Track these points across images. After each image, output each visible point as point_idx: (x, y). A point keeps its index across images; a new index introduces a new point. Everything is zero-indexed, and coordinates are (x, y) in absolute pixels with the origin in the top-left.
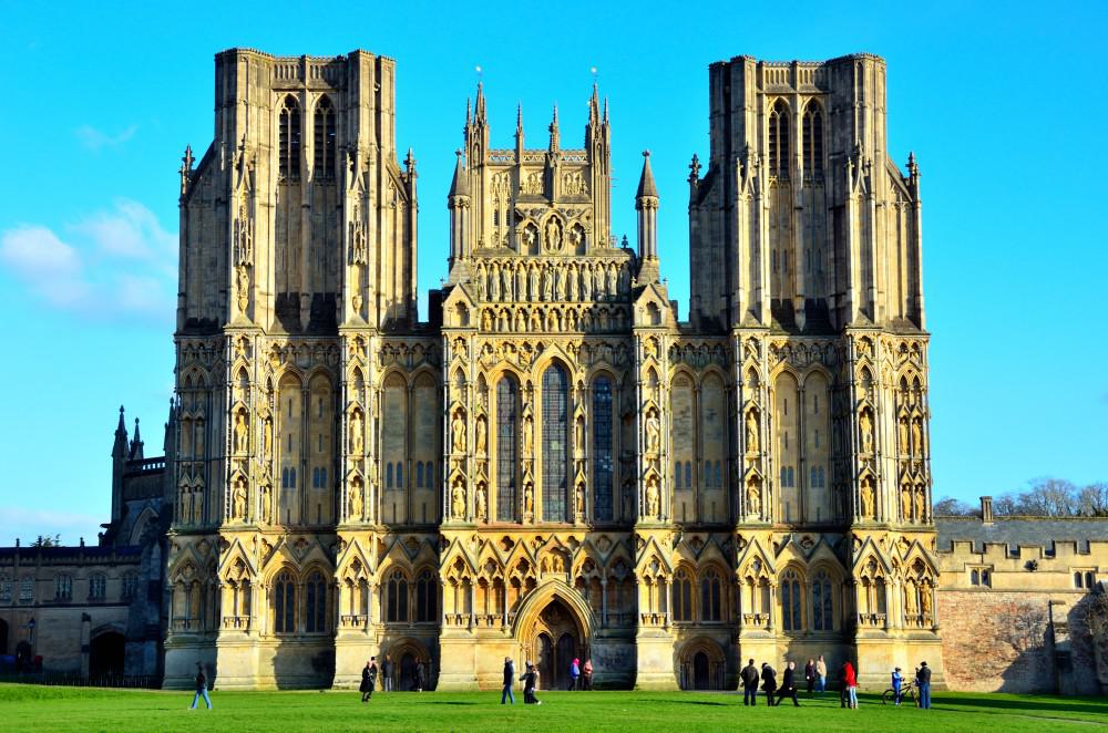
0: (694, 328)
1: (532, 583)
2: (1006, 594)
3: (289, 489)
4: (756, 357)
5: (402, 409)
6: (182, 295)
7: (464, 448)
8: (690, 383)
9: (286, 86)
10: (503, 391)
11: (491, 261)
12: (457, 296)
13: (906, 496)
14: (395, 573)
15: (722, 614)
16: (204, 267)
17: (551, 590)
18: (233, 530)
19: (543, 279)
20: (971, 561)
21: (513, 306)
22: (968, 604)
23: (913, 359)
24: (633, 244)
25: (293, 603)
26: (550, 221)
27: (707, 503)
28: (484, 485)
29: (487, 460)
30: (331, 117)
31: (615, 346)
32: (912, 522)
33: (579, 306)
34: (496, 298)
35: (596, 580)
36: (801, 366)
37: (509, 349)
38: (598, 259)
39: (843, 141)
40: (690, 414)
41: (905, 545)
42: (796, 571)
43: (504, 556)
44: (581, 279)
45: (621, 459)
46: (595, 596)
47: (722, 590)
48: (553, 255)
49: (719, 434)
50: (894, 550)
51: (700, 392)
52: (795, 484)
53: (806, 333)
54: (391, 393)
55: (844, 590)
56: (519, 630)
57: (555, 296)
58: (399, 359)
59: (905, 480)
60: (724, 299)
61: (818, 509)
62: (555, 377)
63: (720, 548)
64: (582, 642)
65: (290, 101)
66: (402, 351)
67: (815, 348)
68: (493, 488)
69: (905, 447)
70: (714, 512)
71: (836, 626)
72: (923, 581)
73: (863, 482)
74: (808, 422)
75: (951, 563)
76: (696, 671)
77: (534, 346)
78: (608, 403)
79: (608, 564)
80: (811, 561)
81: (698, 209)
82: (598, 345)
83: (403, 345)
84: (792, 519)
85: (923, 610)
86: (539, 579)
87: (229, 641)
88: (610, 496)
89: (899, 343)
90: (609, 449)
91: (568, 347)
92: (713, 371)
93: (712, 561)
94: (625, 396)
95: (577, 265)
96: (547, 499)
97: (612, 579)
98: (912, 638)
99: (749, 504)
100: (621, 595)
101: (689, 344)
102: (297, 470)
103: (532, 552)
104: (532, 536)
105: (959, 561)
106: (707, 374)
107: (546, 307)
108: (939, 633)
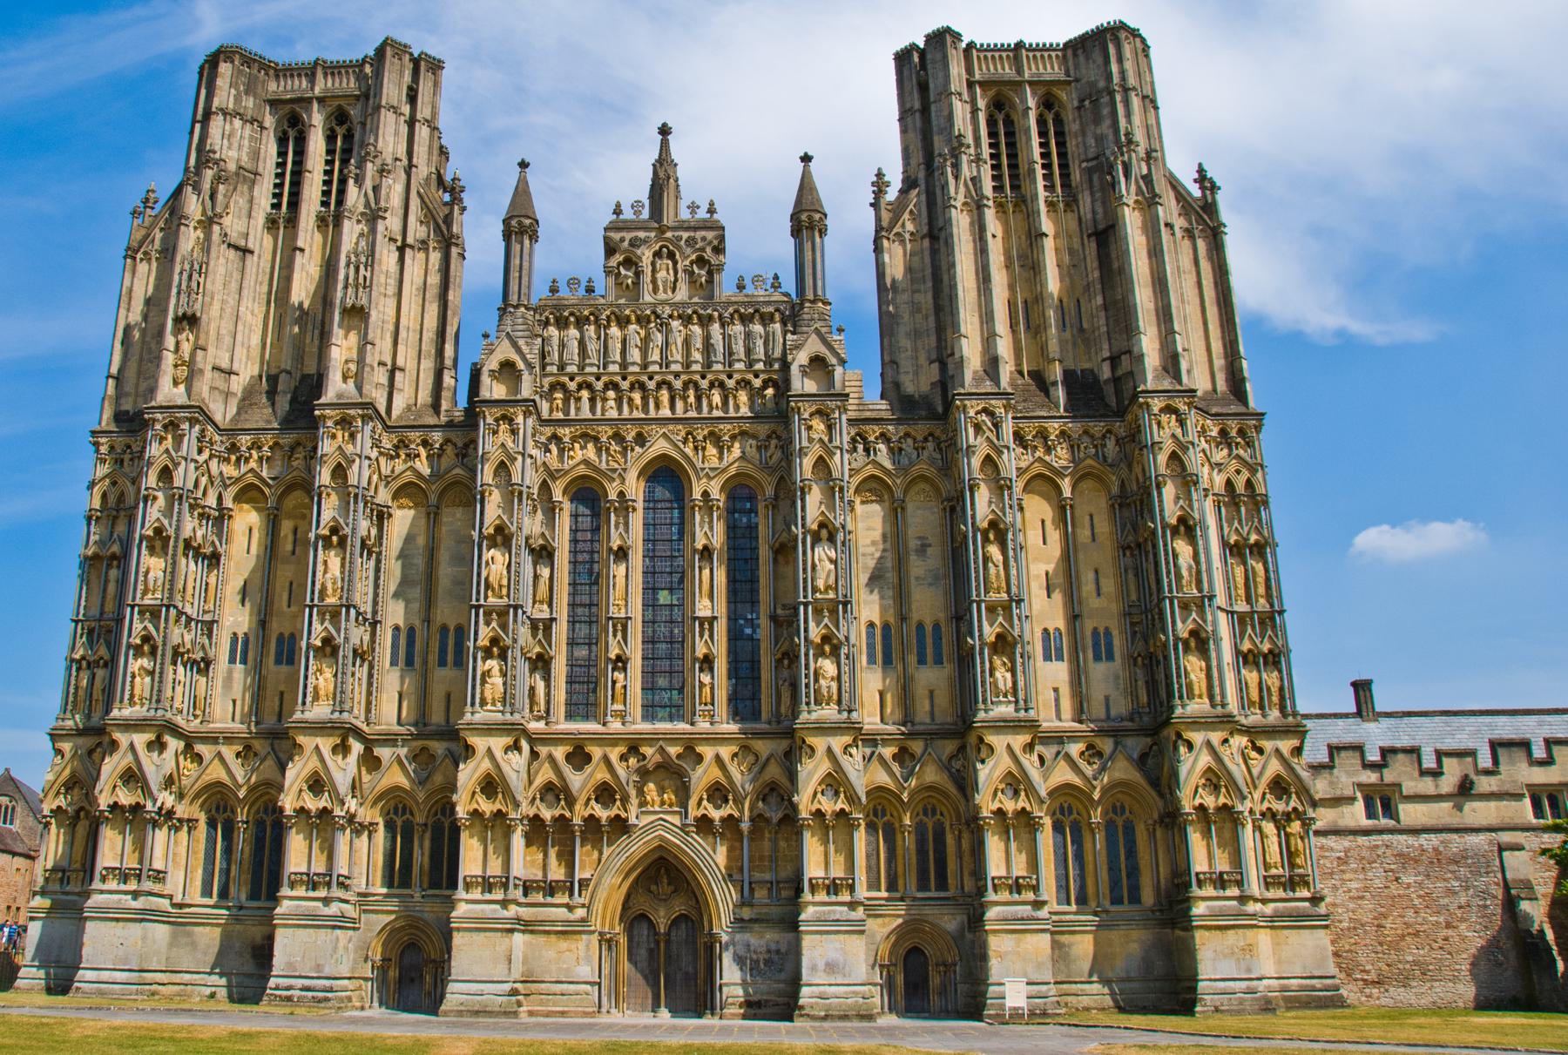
1: (621, 826)
11: (566, 314)
12: (503, 352)
14: (396, 808)
15: (951, 881)
19: (646, 340)
22: (1365, 853)
23: (1241, 452)
24: (789, 285)
26: (658, 254)
27: (920, 692)
28: (541, 663)
29: (553, 620)
30: (348, 137)
31: (763, 436)
32: (1264, 716)
35: (730, 821)
37: (590, 446)
39: (1100, 139)
41: (1253, 754)
42: (1076, 805)
44: (707, 338)
45: (774, 618)
47: (950, 840)
49: (936, 578)
51: (903, 508)
55: (1159, 833)
57: (665, 363)
59: (1246, 646)
60: (936, 366)
61: (1107, 699)
63: (946, 767)
66: (423, 452)
67: (1086, 439)
68: (560, 668)
69: (1242, 592)
70: (932, 706)
71: (1148, 897)
74: (1081, 556)
75: (1331, 783)
76: (906, 983)
77: (629, 438)
78: (752, 528)
82: (733, 437)
85: (1292, 865)
88: (756, 679)
90: (754, 603)
91: (685, 441)
92: (923, 478)
93: (930, 788)
94: (780, 518)
96: (649, 688)
97: (757, 819)
98: (1277, 916)
99: (995, 684)
100: (775, 849)
104: (622, 749)
105: (1344, 779)
106: (913, 482)
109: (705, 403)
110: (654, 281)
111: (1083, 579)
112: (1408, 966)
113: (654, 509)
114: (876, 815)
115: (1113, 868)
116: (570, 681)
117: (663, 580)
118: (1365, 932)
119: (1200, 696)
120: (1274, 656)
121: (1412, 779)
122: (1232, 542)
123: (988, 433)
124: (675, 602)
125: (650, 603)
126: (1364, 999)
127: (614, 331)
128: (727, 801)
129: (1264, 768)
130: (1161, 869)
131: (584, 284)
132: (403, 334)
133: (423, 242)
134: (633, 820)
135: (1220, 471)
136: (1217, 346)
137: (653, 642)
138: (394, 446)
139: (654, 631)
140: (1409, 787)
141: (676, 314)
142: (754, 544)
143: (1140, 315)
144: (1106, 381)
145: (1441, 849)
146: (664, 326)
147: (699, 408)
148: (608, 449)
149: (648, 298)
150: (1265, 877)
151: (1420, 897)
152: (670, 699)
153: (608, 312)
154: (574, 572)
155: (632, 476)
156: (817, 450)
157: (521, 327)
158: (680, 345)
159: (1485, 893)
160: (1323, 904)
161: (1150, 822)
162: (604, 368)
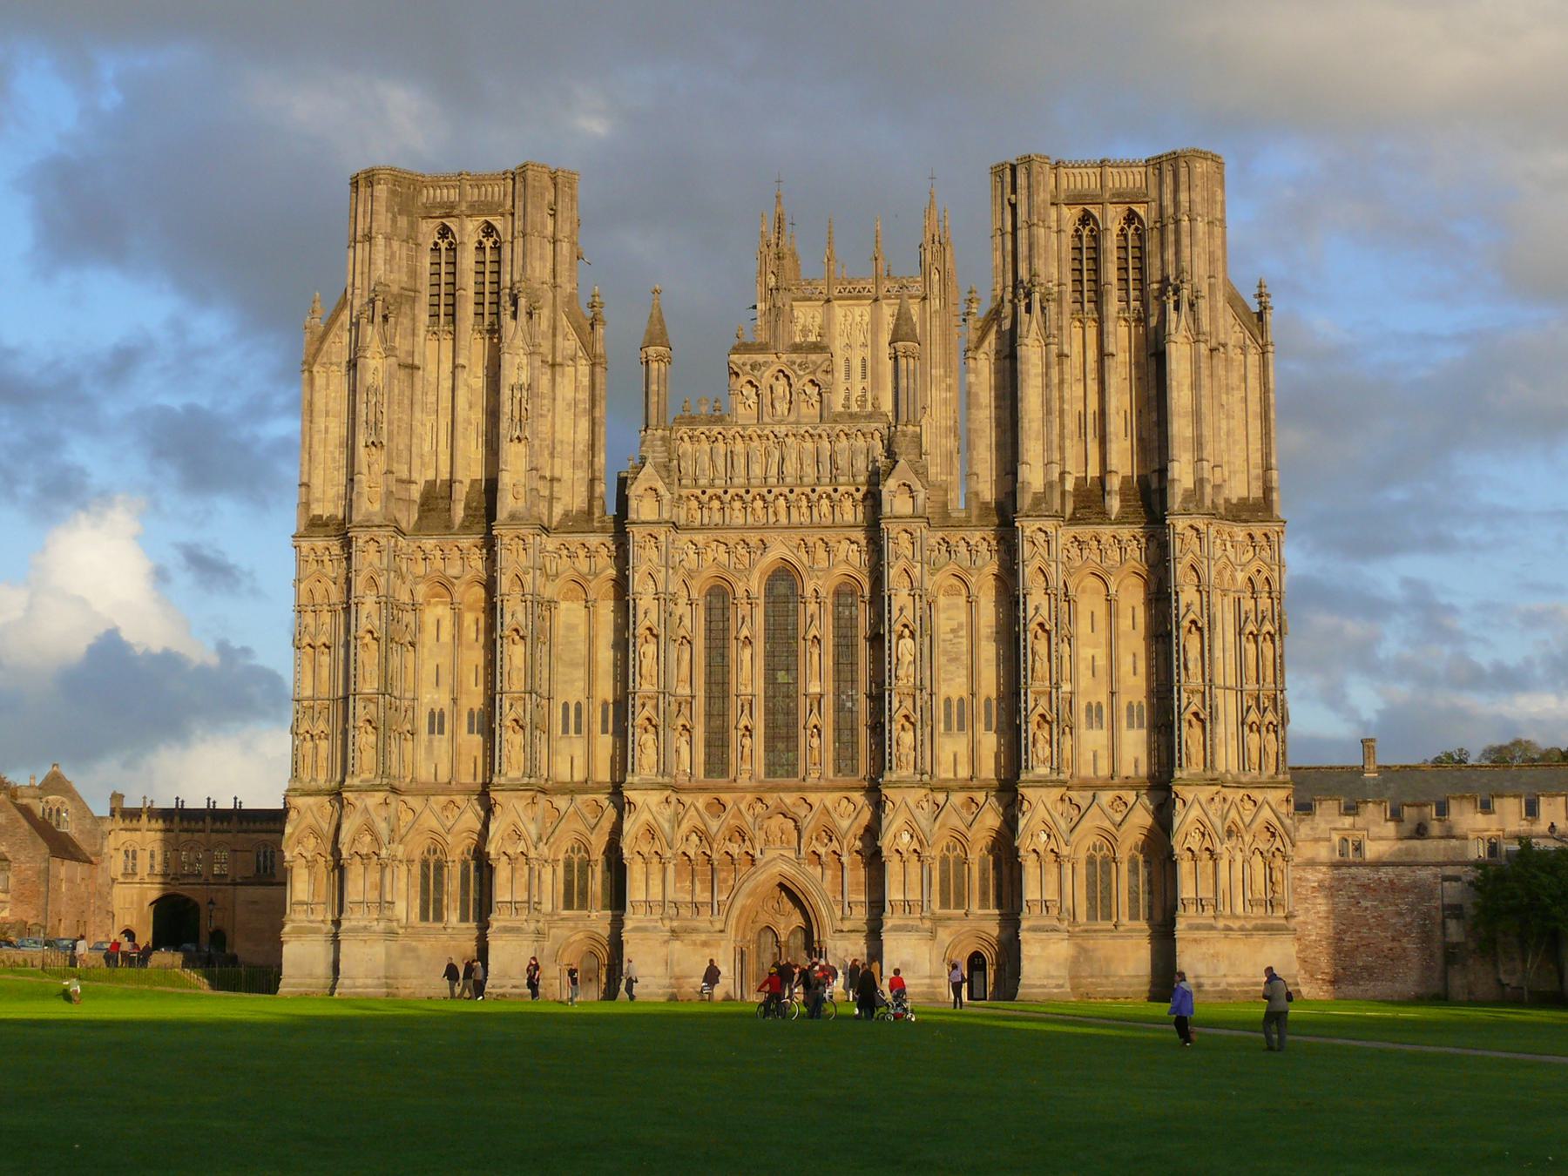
0: (969, 516)
2: (1384, 870)
3: (437, 736)
4: (1046, 556)
5: (582, 630)
8: (964, 592)
9: (437, 213)
10: (713, 606)
13: (1253, 740)
16: (331, 449)
17: (776, 870)
18: (359, 790)
20: (1339, 825)
21: (726, 492)
25: (442, 884)
29: (693, 697)
30: (497, 248)
33: (813, 491)
34: (703, 482)
36: (1112, 566)
40: (963, 633)
41: (1249, 805)
43: (714, 825)
46: (834, 877)
48: (780, 422)
52: (1105, 725)
53: (1120, 521)
54: (568, 609)
56: (732, 921)
58: (577, 564)
60: (1009, 477)
61: (1136, 761)
62: (782, 589)
64: (816, 938)
65: (445, 232)
66: (582, 553)
69: (1253, 673)
72: (1273, 853)
74: (1122, 643)
75: (1312, 829)
78: (853, 619)
79: (850, 834)
81: (975, 359)
84: (1100, 773)
86: (758, 855)
87: (354, 930)
88: (854, 744)
89: (1242, 534)
90: (853, 681)
95: (811, 435)
96: (770, 747)
98: (1256, 928)
102: (446, 714)
103: (750, 819)
104: (750, 797)
105: (1323, 826)
107: (770, 492)
108: (1293, 923)
109: (815, 510)
111: (1122, 661)
112: (1358, 970)
114: (948, 849)
116: (708, 744)
120: (1274, 726)
121: (1378, 824)
122: (1247, 632)
124: (791, 681)
125: (770, 679)
126: (1321, 994)
127: (739, 447)
128: (831, 840)
130: (1168, 894)
132: (558, 448)
135: (1242, 571)
136: (1256, 457)
137: (774, 714)
139: (774, 705)
140: (1374, 830)
141: (790, 434)
142: (854, 631)
143: (1176, 444)
144: (1155, 490)
145: (1396, 881)
146: (781, 443)
151: (1373, 917)
152: (787, 760)
153: (732, 432)
154: (709, 657)
155: (756, 575)
156: (902, 563)
158: (794, 460)
159: (1427, 915)
161: (1161, 857)
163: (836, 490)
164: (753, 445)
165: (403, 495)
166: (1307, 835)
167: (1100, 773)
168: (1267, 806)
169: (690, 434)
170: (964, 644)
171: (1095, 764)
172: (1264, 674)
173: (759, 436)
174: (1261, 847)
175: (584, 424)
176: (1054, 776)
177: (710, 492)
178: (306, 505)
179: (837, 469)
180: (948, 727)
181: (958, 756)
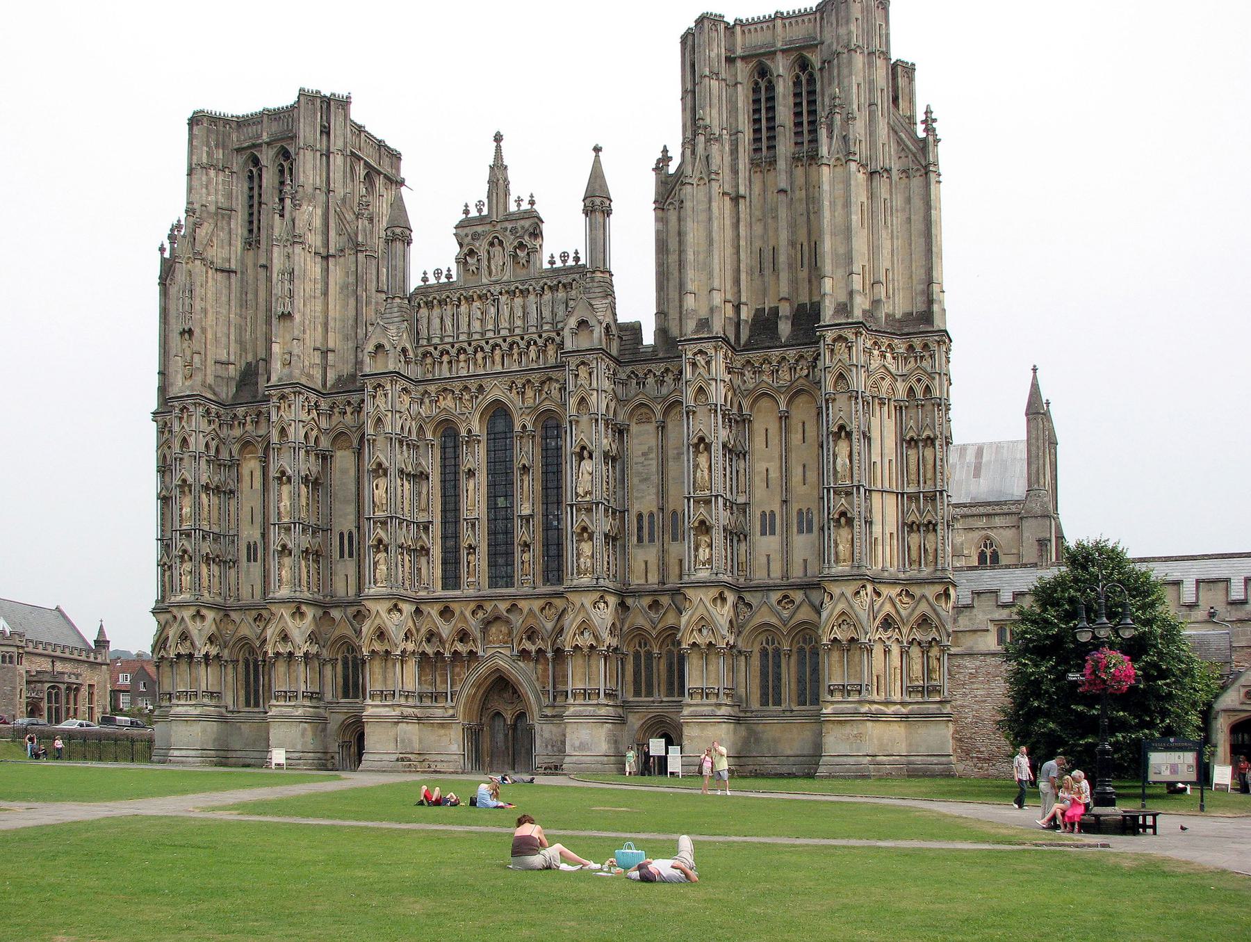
4: (707, 376)
5: (352, 472)
6: (162, 373)
7: (385, 508)
10: (447, 445)
21: (453, 347)
26: (492, 244)
28: (425, 551)
34: (436, 341)
38: (541, 284)
40: (653, 455)
41: (906, 600)
43: (445, 629)
50: (888, 608)
51: (663, 427)
54: (341, 457)
57: (497, 330)
61: (805, 561)
62: (500, 426)
66: (349, 410)
68: (436, 552)
73: (838, 521)
78: (558, 448)
80: (790, 624)
82: (543, 383)
83: (349, 403)
85: (930, 678)
90: (559, 503)
95: (521, 291)
101: (650, 371)
104: (473, 606)
108: (947, 709)
110: (489, 267)
113: (494, 439)
114: (640, 646)
115: (801, 681)
117: (500, 489)
118: (984, 726)
119: (844, 561)
123: (701, 370)
125: (492, 506)
129: (913, 610)
131: (445, 272)
132: (331, 324)
133: (342, 251)
134: (480, 653)
137: (495, 534)
138: (330, 407)
139: (496, 527)
147: (520, 363)
148: (460, 398)
149: (485, 281)
150: (908, 687)
152: (506, 573)
153: (458, 295)
154: (444, 488)
157: (396, 315)
160: (948, 706)
162: (458, 337)
163: (540, 337)
164: (474, 304)
165: (225, 374)
166: (965, 626)
167: (772, 575)
168: (924, 600)
169: (425, 300)
170: (653, 465)
171: (769, 568)
172: (925, 476)
173: (480, 297)
174: (918, 637)
175: (352, 302)
176: (714, 577)
177: (439, 347)
178: (163, 389)
179: (542, 318)
180: (640, 539)
181: (648, 565)
